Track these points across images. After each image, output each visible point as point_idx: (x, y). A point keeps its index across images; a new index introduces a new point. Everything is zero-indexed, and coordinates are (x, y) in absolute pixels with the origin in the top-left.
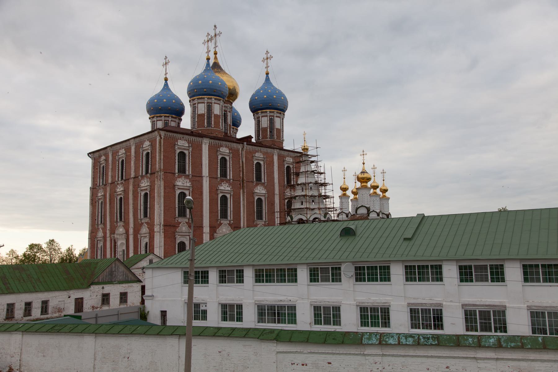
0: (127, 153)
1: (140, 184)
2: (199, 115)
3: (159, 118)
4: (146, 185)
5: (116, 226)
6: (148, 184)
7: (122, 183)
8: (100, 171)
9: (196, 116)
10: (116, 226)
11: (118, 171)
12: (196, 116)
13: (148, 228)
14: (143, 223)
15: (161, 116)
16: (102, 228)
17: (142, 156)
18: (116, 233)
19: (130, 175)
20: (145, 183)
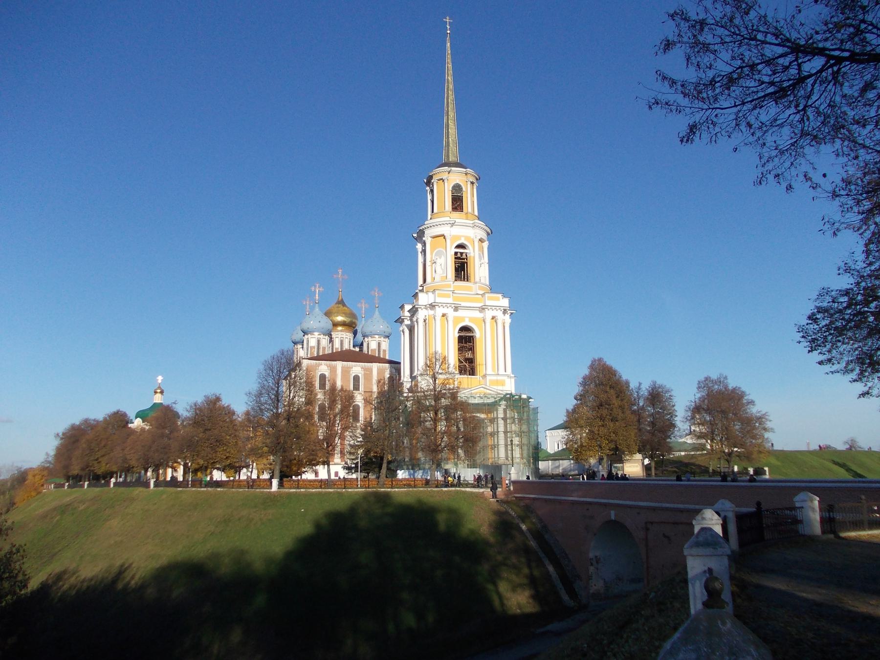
3: (324, 337)
19: (372, 389)
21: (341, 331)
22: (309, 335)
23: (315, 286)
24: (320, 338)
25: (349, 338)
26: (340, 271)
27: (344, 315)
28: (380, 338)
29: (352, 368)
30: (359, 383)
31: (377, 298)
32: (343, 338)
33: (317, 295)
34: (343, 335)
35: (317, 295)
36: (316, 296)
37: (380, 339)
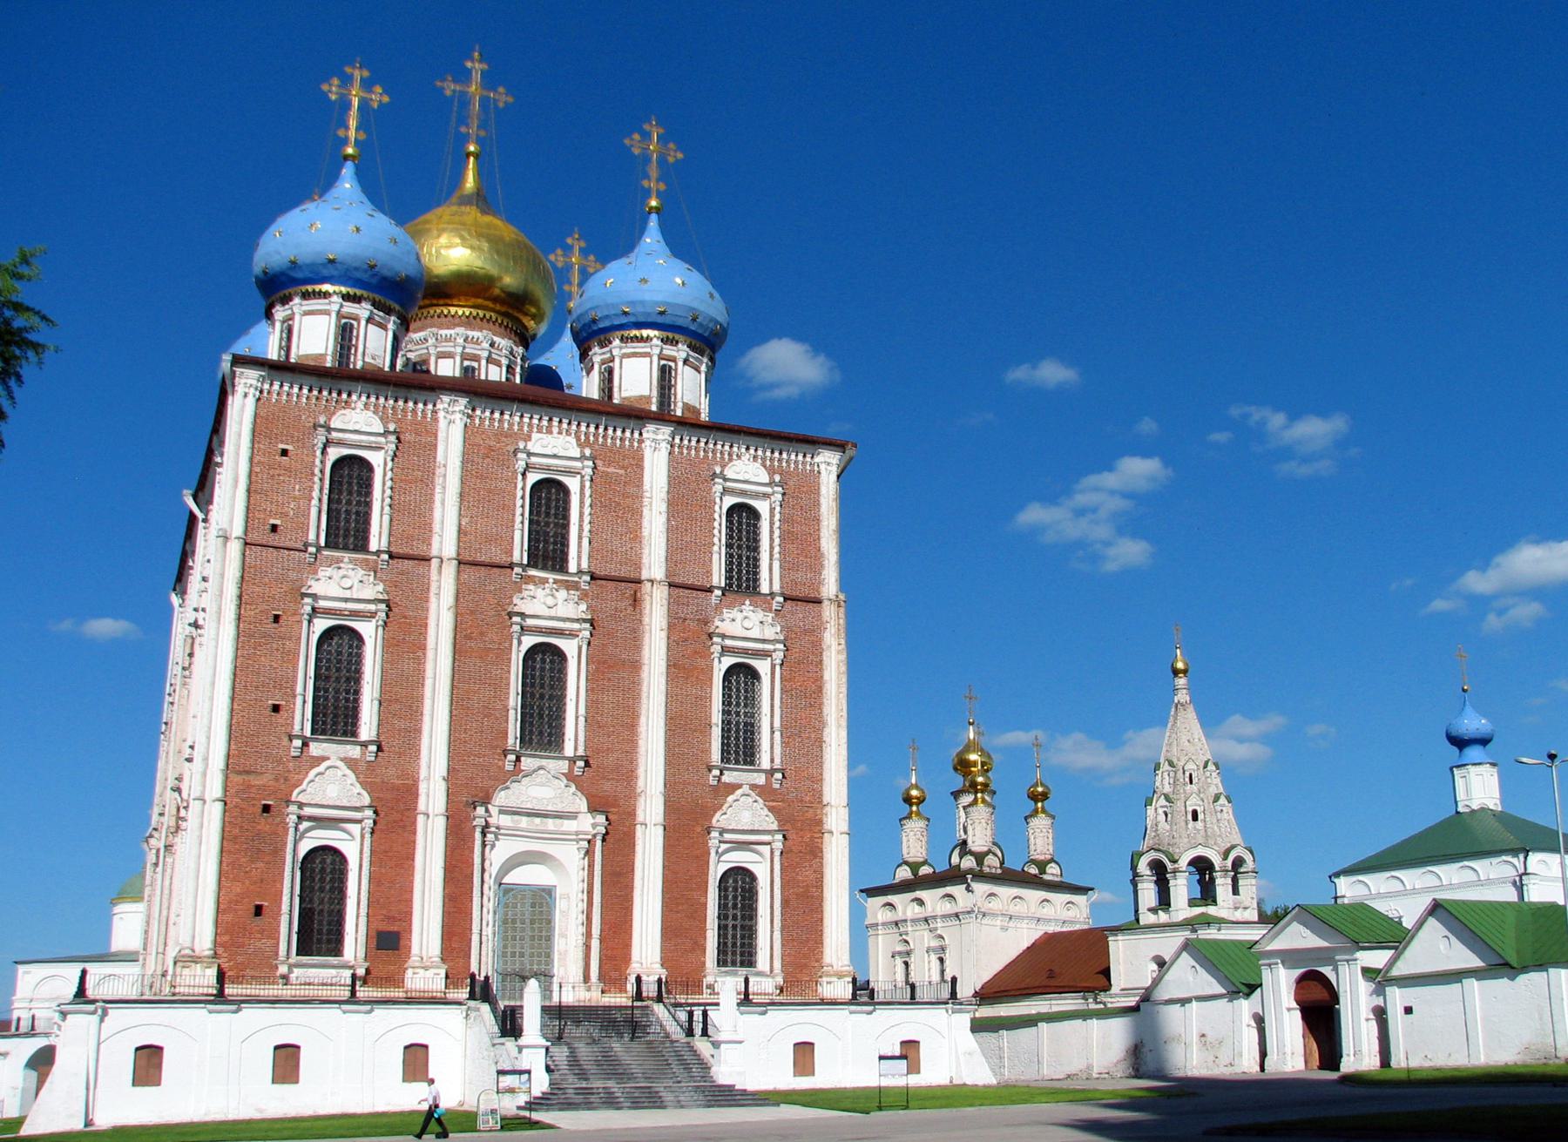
0: (599, 463)
1: (717, 623)
2: (686, 407)
4: (755, 633)
5: (509, 767)
6: (771, 632)
7: (569, 586)
8: (322, 472)
9: (680, 405)
10: (511, 768)
11: (522, 523)
12: (680, 405)
13: (771, 809)
14: (733, 788)
15: (388, 311)
16: (351, 763)
17: (721, 508)
18: (501, 798)
19: (638, 566)
20: (747, 624)
21: (468, 322)
22: (297, 300)
23: (346, 80)
24: (357, 319)
25: (505, 362)
26: (476, 67)
27: (485, 246)
28: (674, 342)
29: (528, 438)
30: (566, 526)
31: (653, 171)
32: (476, 358)
33: (353, 123)
34: (477, 343)
35: (353, 123)
36: (347, 128)
37: (669, 351)
